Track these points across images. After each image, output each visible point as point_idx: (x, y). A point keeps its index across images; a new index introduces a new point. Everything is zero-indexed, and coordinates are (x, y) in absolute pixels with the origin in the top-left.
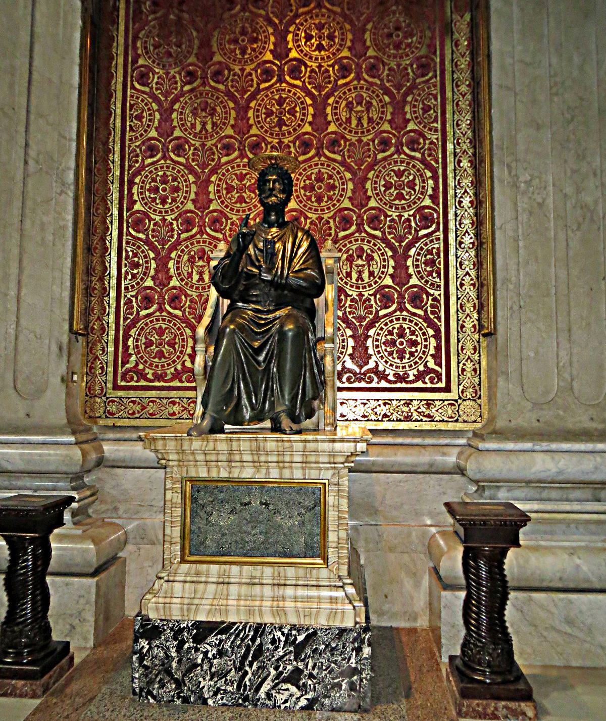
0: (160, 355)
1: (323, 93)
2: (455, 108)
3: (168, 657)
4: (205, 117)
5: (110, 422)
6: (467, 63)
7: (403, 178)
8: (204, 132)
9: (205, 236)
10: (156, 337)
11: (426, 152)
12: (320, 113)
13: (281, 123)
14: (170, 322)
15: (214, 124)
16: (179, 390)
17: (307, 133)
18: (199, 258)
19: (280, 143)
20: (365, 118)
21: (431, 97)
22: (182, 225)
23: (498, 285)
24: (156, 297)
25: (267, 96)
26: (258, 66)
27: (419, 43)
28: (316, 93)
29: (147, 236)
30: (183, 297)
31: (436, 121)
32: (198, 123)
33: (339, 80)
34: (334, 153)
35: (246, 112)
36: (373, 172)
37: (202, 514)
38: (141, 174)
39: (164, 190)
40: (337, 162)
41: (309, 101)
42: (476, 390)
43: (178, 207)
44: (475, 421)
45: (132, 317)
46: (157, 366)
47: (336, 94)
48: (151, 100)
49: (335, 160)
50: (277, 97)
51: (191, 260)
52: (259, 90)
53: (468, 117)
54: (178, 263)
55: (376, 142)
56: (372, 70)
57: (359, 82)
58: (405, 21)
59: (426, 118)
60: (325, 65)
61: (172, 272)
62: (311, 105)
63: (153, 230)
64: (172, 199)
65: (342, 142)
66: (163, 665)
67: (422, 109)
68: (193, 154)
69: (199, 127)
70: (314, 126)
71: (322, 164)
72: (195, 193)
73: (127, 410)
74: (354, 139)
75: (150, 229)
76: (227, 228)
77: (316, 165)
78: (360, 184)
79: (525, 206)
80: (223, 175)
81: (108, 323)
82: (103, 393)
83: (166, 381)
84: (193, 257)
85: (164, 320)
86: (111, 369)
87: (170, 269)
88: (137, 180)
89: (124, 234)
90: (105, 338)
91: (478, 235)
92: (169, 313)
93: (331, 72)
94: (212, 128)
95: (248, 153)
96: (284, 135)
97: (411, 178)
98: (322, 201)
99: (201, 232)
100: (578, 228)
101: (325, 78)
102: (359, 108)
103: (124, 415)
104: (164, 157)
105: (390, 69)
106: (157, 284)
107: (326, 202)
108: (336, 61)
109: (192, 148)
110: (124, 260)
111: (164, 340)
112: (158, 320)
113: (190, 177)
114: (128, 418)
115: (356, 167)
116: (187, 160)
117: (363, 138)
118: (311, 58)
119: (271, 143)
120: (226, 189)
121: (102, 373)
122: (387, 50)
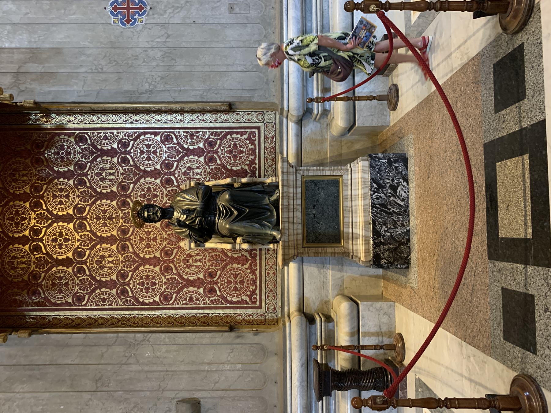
0: (242, 282)
1: (94, 194)
2: (105, 123)
4: (105, 262)
6: (80, 116)
7: (144, 150)
8: (114, 262)
11: (130, 138)
12: (106, 196)
13: (111, 218)
14: (223, 277)
15: (110, 256)
17: (117, 203)
18: (188, 262)
19: (122, 218)
20: (109, 171)
21: (99, 135)
23: (205, 100)
24: (210, 286)
25: (94, 226)
26: (76, 232)
27: (68, 141)
28: (94, 198)
29: (174, 293)
30: (210, 270)
31: (112, 133)
32: (109, 266)
33: (87, 186)
34: (129, 188)
35: (103, 237)
36: (141, 167)
37: (320, 237)
38: (138, 298)
39: (147, 284)
41: (99, 202)
43: (158, 276)
44: (275, 114)
45: (221, 300)
46: (248, 284)
47: (95, 187)
48: (94, 294)
50: (95, 220)
51: (189, 266)
52: (91, 231)
53: (111, 116)
54: (190, 274)
55: (123, 165)
56: (82, 167)
57: (88, 175)
58: (54, 150)
59: (111, 138)
60: (78, 193)
61: (195, 278)
62: (101, 201)
63: (171, 289)
65: (123, 184)
66: (392, 252)
67: (105, 140)
68: (127, 268)
69: (111, 265)
70: (114, 199)
71: (136, 194)
73: (273, 300)
74: (122, 177)
75: (170, 291)
76: (171, 247)
78: (146, 174)
79: (162, 86)
80: (140, 250)
81: (224, 314)
82: (263, 315)
83: (256, 278)
84: (187, 266)
85: (222, 281)
86: (250, 311)
88: (141, 300)
89: (173, 306)
90: (233, 315)
91: (176, 112)
92: (218, 278)
93: (82, 190)
94: (112, 257)
95: (128, 236)
96: (118, 216)
97: (144, 146)
98: (157, 194)
99: (173, 262)
100: (175, 60)
101: (86, 193)
102: (104, 174)
103: (276, 302)
104: (128, 285)
105: (82, 158)
107: (157, 192)
108: (75, 187)
109: (123, 268)
110: (188, 306)
111: (234, 280)
112: (222, 284)
113: (140, 269)
115: (138, 176)
116: (130, 271)
118: (73, 202)
119: (122, 223)
120: (148, 248)
122: (70, 159)
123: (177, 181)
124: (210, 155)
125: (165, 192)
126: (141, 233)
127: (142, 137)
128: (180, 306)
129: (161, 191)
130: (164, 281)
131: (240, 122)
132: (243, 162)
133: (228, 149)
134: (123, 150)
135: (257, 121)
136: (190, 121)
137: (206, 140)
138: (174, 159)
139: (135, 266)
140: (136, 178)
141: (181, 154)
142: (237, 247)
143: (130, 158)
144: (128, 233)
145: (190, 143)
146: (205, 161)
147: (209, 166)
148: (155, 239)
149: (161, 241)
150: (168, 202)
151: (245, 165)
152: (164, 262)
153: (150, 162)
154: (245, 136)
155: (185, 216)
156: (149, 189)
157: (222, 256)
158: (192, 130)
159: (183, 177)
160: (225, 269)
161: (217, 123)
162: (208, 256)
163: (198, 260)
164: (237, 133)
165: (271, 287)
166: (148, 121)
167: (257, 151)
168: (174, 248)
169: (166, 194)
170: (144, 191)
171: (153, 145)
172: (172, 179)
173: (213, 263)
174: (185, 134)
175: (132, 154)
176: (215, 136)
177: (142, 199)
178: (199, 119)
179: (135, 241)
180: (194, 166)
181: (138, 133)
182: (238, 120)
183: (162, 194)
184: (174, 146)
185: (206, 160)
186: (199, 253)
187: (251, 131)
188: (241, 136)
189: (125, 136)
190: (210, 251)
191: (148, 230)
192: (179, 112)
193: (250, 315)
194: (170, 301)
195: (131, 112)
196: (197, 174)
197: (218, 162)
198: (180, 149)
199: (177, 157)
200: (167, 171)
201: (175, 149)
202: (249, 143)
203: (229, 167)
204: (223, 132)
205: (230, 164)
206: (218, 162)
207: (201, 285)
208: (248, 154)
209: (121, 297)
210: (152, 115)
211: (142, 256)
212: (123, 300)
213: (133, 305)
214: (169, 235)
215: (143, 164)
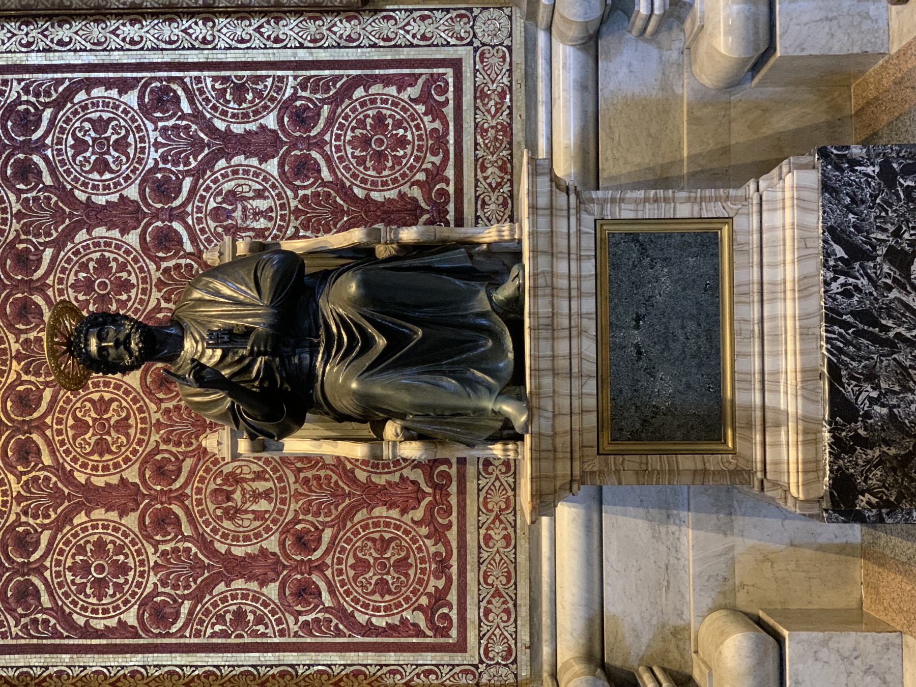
0: (402, 565)
3: (881, 462)
5: (524, 657)
7: (87, 138)
9: (188, 491)
10: (371, 574)
11: (42, 99)
14: (343, 550)
16: (465, 531)
18: (229, 499)
19: (19, 357)
22: (168, 533)
24: (299, 577)
29: (184, 597)
30: (299, 527)
34: (40, 261)
36: (77, 192)
37: (657, 422)
39: (100, 569)
40: (58, 254)
42: (457, 16)
43: (133, 542)
44: (510, 18)
45: (335, 621)
46: (423, 571)
49: (54, 259)
51: (232, 514)
55: (21, 186)
63: (175, 587)
64: (117, 555)
65: (21, 246)
68: (35, 516)
71: (61, 281)
72: (107, 511)
73: (502, 625)
74: (16, 226)
75: (172, 592)
76: (174, 450)
77: (61, 292)
80: (75, 460)
81: (345, 665)
82: (472, 670)
83: (449, 553)
84: (226, 511)
85: (340, 561)
86: (429, 658)
87: (247, 553)
88: (81, 621)
89: (182, 641)
90: (373, 670)
92: (327, 552)
95: (36, 415)
97: (87, 125)
98: (128, 281)
99: (181, 498)
103: (511, 629)
106: (274, 577)
107: (129, 274)
109: (23, 519)
110: (229, 641)
111: (375, 559)
112: (340, 572)
113: (76, 521)
114: (516, 621)
115: (67, 221)
116: (44, 527)
117: (14, 211)
119: (18, 374)
120: (101, 455)
121: (435, 673)
123: (194, 239)
124: (297, 152)
125: (156, 275)
126: (78, 405)
127: (81, 96)
128: (205, 641)
129: (141, 269)
130: (153, 559)
131: (395, 46)
132: (404, 175)
133: (358, 132)
134: (22, 138)
135: (453, 41)
136: (234, 44)
137: (286, 106)
138: (181, 168)
139: (59, 511)
140: (60, 230)
141: (206, 151)
142: (387, 453)
143: (42, 164)
144: (38, 405)
145: (234, 116)
146: (282, 173)
147: (295, 189)
148: (122, 426)
149: (143, 432)
150: (164, 305)
151: (413, 184)
152: (153, 498)
153: (107, 176)
154: (413, 92)
155: (219, 352)
156: (103, 264)
157: (336, 482)
158: (240, 73)
159: (212, 225)
160: (349, 525)
161: (320, 47)
162: (292, 480)
163: (260, 494)
164: (387, 81)
165: (497, 583)
166: (99, 43)
167: (451, 139)
168: (185, 455)
169: (159, 279)
170: (88, 272)
171: (114, 123)
172: (176, 232)
173: (310, 503)
174: (217, 86)
175: (49, 153)
176: (315, 91)
177: (81, 297)
178: (262, 34)
179: (59, 432)
180: (246, 188)
181: (67, 83)
182: (388, 39)
183: (144, 280)
184: (184, 123)
185: (287, 168)
186: (265, 471)
187: (432, 75)
188: (399, 92)
189: (27, 92)
190: (299, 465)
191: (102, 397)
192: (199, 13)
193: (431, 672)
194: (173, 623)
195: (44, 16)
196: (257, 214)
197: (326, 174)
198: (202, 135)
199: (191, 159)
200: (159, 206)
201: (187, 134)
202: (425, 114)
203: (359, 193)
204: (342, 76)
205: (364, 181)
206: (326, 174)
207: (271, 575)
208: (420, 148)
209: (15, 610)
210: (113, 24)
211: (81, 478)
212: (23, 621)
213: (56, 634)
214: (167, 411)
215: (85, 184)
